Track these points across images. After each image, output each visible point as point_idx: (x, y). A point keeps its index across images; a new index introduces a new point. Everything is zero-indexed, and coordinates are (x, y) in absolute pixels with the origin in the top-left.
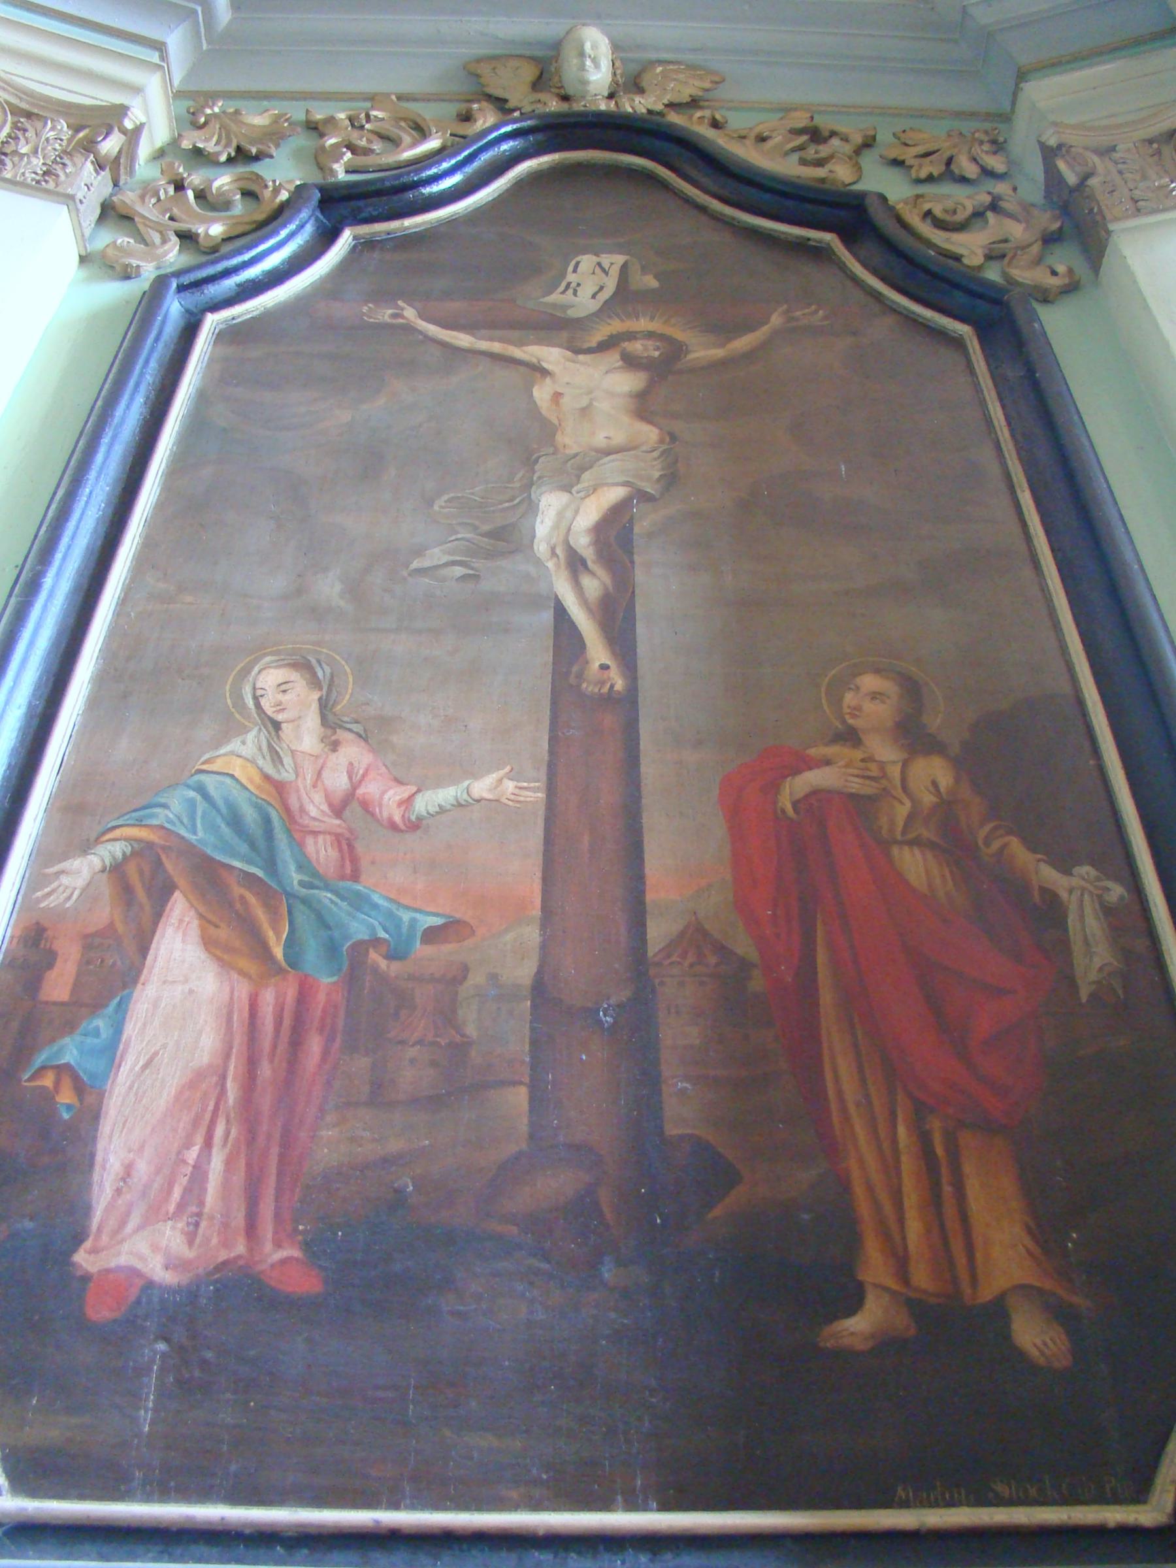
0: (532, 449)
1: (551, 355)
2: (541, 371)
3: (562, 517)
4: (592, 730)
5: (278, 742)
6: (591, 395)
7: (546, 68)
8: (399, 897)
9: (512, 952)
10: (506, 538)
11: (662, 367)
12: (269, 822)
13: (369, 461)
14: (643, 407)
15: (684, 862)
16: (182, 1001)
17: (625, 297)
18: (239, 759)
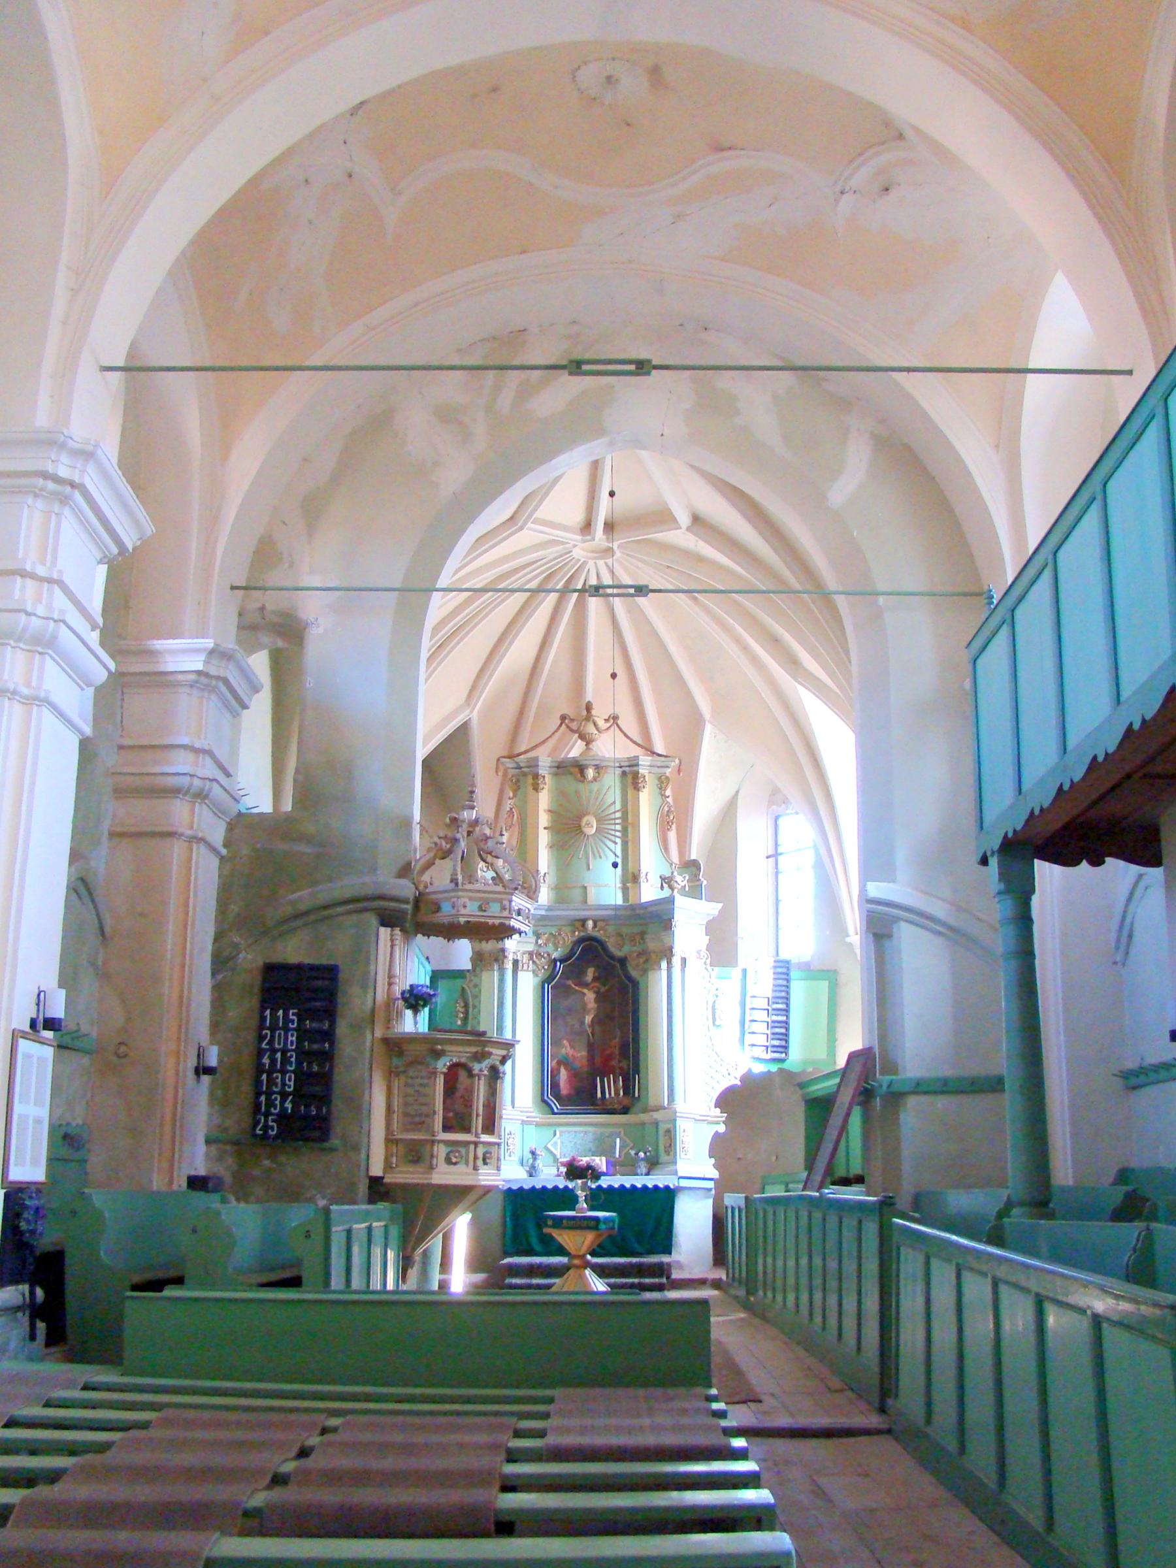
0: (584, 1005)
1: (585, 991)
2: (584, 994)
3: (588, 1019)
4: (591, 1047)
5: (566, 1049)
6: (590, 996)
7: (583, 922)
8: (577, 1065)
9: (586, 1069)
10: (583, 1023)
11: (597, 993)
12: (566, 1057)
13: (570, 1010)
14: (596, 1000)
15: (598, 1059)
16: (563, 1074)
17: (595, 979)
18: (563, 1051)
